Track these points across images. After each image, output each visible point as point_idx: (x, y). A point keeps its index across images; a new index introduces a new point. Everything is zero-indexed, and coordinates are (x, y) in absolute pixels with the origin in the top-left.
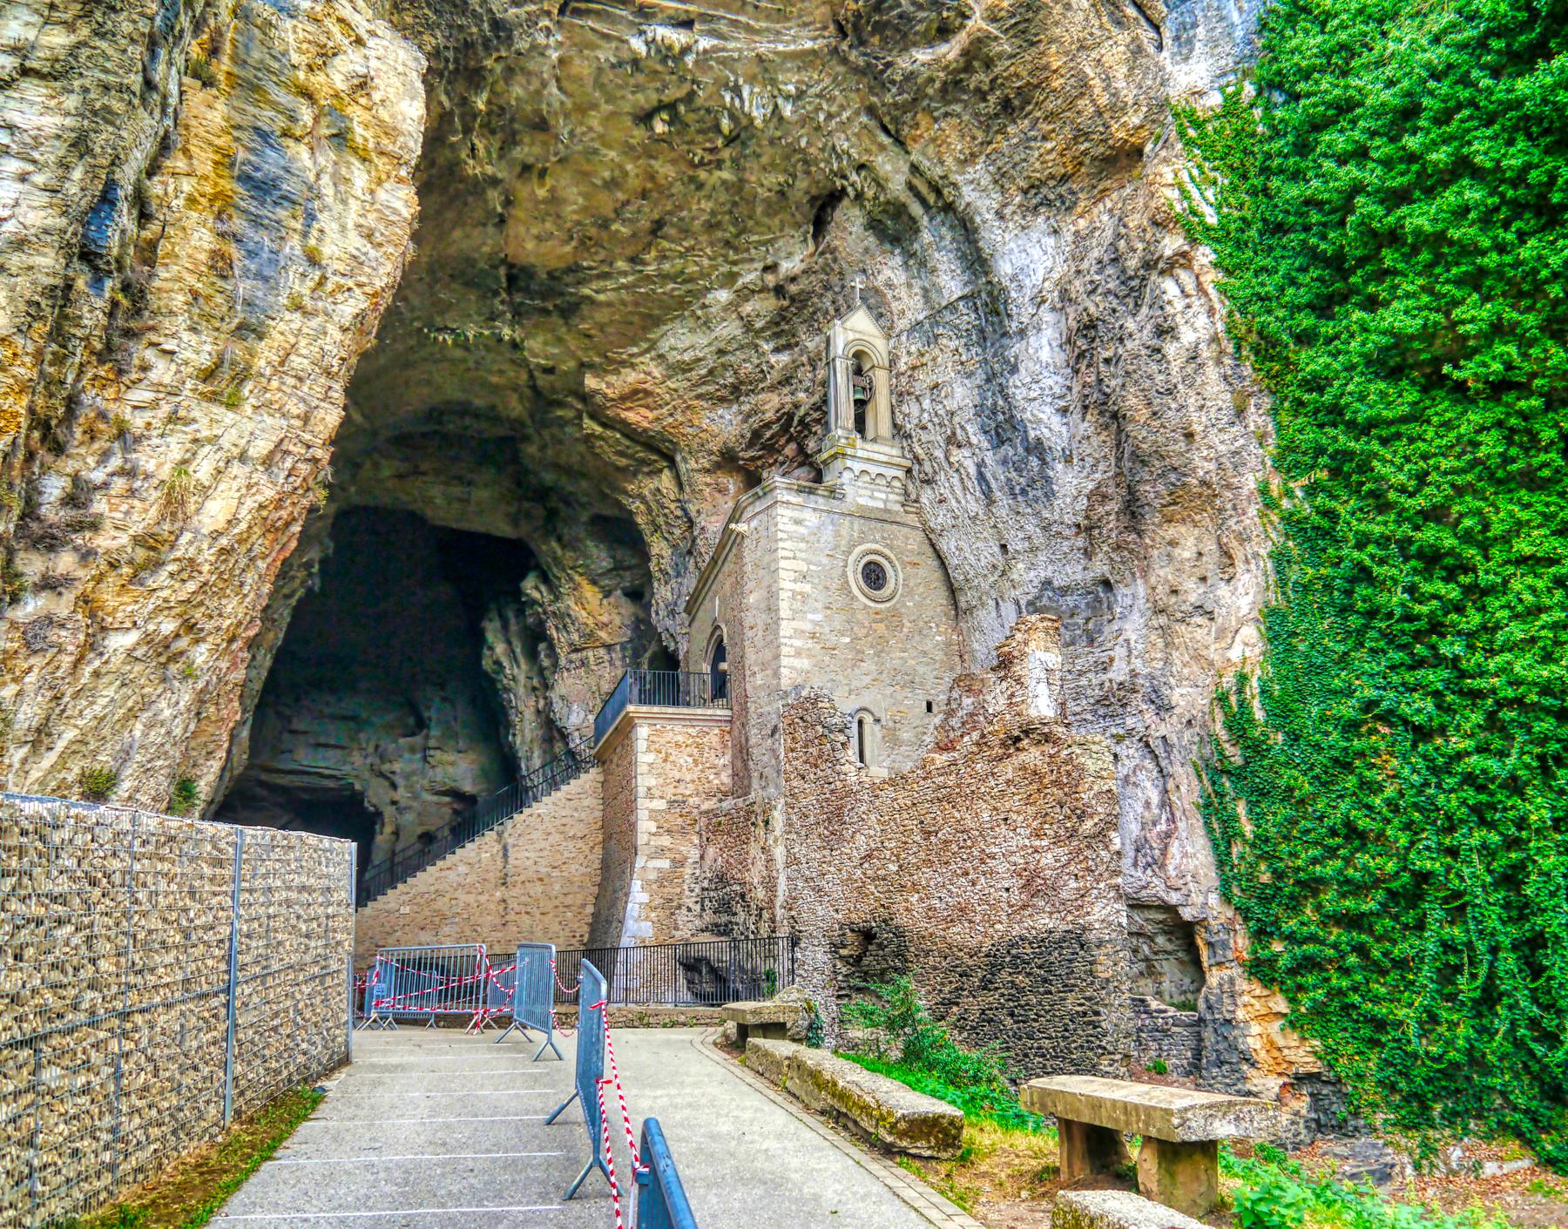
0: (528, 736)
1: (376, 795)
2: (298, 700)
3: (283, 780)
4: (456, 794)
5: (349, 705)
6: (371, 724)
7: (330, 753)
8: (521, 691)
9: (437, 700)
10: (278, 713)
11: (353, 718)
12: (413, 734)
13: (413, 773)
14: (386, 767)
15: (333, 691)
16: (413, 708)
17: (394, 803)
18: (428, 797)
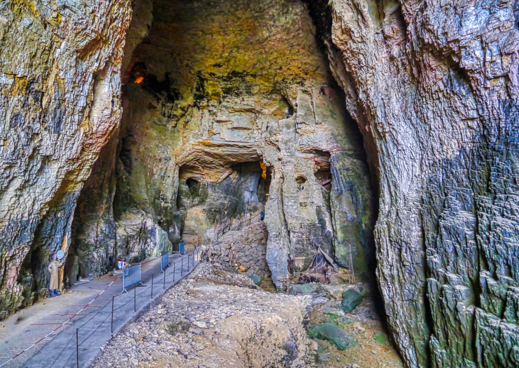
0: (382, 85)
1: (270, 156)
2: (220, 102)
3: (219, 151)
4: (319, 152)
5: (250, 101)
7: (242, 132)
8: (371, 46)
9: (299, 92)
10: (209, 111)
11: (250, 111)
12: (288, 117)
13: (289, 140)
14: (273, 138)
15: (237, 95)
16: (285, 100)
17: (280, 160)
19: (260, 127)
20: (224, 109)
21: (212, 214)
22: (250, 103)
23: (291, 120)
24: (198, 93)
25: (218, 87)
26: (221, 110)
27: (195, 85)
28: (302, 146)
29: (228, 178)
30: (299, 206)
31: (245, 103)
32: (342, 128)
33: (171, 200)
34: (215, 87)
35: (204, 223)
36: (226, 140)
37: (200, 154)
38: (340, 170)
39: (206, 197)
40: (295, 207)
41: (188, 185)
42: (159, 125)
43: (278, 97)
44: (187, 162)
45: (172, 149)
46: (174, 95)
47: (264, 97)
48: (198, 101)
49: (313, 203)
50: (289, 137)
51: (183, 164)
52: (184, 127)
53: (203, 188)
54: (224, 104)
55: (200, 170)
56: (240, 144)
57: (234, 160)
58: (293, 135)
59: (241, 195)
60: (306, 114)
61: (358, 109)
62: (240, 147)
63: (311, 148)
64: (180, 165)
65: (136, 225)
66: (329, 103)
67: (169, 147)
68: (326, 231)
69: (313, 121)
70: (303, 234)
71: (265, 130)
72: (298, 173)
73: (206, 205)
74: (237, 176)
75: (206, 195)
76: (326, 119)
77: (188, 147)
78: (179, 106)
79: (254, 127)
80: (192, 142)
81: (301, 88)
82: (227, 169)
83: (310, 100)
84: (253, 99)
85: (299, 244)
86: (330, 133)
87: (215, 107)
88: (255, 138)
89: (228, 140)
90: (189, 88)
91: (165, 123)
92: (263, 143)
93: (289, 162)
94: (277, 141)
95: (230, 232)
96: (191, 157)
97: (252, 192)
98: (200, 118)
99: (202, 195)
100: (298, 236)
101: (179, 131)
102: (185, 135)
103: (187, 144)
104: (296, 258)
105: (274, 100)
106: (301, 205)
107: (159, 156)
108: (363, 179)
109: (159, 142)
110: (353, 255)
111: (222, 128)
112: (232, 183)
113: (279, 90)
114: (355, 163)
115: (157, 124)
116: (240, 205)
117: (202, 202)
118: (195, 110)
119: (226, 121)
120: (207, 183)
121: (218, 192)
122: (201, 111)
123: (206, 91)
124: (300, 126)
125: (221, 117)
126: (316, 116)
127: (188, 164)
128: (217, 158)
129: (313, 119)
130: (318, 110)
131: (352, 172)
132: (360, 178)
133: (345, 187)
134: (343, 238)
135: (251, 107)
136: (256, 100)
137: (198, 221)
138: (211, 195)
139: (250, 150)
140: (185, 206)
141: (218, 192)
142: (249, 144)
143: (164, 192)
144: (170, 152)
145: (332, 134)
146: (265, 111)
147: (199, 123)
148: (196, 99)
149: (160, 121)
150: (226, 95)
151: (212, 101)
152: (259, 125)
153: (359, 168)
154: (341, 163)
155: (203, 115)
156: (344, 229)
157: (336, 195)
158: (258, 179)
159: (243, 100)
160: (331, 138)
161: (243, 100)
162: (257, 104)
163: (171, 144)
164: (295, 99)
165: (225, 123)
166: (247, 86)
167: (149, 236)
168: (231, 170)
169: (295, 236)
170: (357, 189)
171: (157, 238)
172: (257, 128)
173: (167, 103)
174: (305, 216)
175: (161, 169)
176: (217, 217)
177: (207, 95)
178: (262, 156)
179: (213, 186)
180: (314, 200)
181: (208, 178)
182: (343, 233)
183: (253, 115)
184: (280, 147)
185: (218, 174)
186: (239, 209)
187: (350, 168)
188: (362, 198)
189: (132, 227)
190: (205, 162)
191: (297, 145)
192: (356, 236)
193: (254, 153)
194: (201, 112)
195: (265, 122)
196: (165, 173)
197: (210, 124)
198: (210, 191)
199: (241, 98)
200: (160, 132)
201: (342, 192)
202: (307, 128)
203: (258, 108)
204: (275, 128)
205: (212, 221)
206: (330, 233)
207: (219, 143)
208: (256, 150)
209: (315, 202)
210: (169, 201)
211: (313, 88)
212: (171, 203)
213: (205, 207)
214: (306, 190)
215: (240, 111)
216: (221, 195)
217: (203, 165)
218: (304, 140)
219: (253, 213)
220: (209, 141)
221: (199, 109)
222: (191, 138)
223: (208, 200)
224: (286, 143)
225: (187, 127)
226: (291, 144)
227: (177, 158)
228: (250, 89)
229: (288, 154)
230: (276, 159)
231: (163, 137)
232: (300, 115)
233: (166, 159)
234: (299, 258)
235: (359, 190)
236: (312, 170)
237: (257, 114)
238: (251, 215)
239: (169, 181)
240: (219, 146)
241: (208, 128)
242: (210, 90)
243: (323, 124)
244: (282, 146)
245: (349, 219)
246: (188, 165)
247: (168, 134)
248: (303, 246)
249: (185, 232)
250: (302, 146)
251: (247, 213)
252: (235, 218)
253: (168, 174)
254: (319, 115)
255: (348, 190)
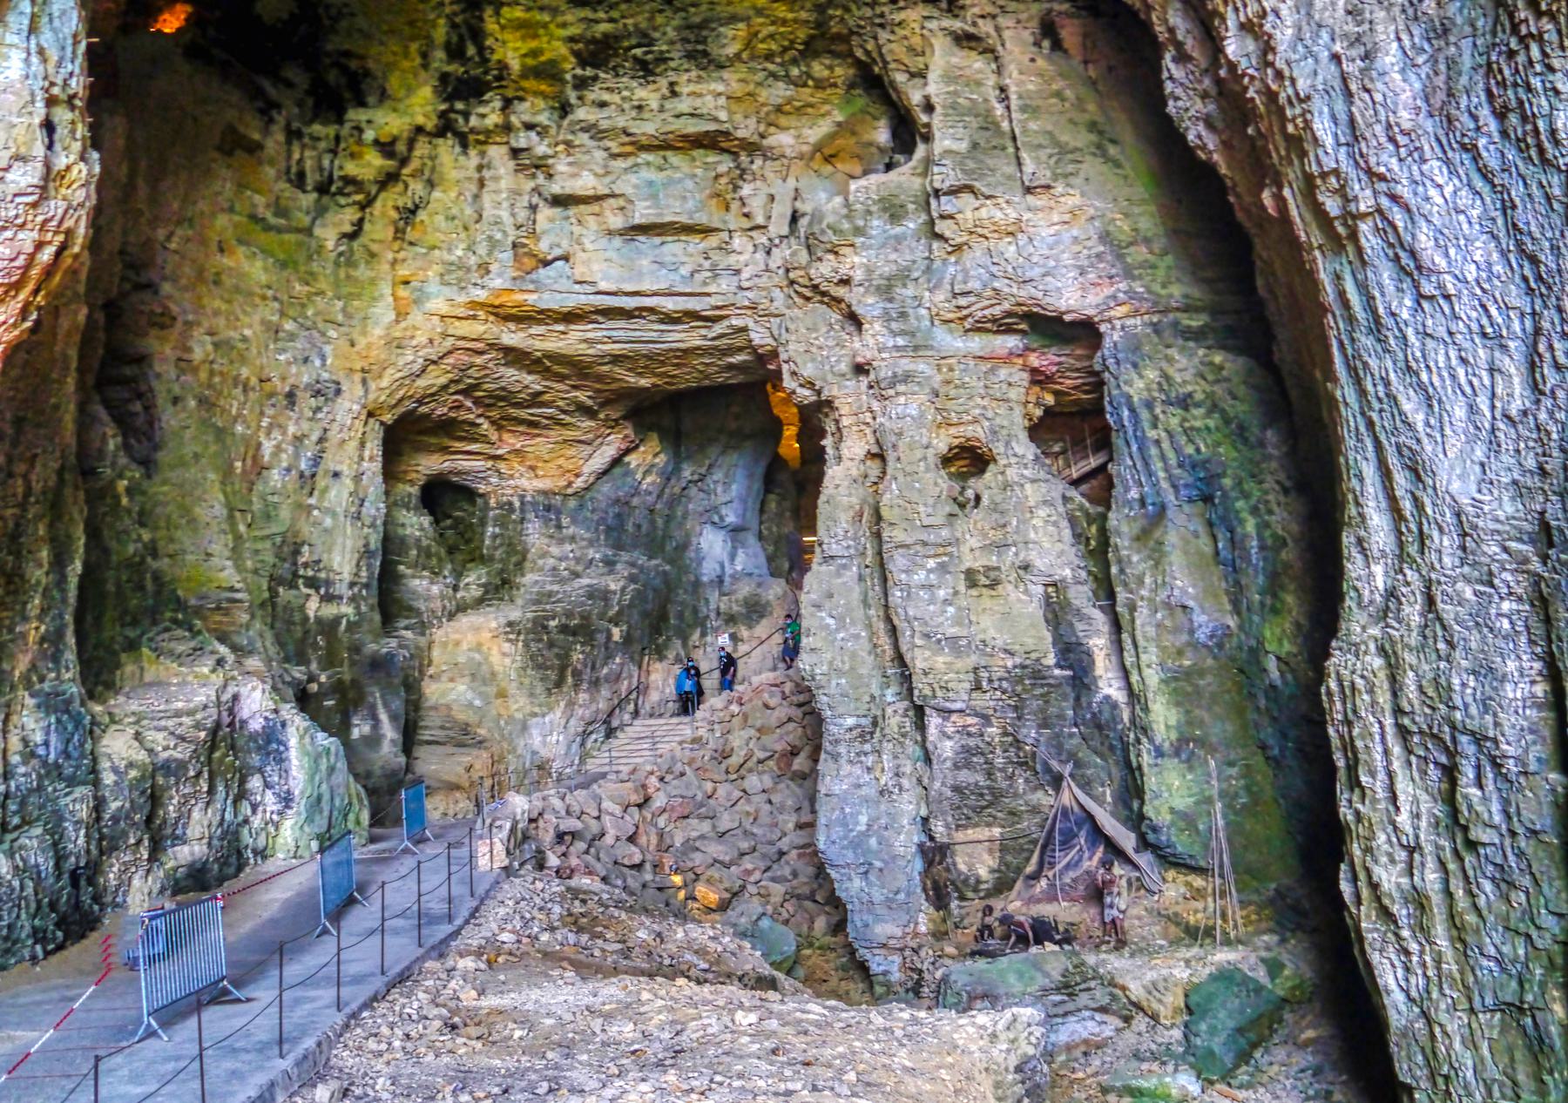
1: (811, 355)
2: (564, 109)
3: (570, 341)
4: (1046, 327)
5: (707, 98)
6: (767, 154)
7: (674, 248)
9: (940, 44)
10: (515, 153)
12: (889, 167)
13: (903, 276)
14: (825, 269)
15: (647, 70)
16: (873, 83)
17: (860, 369)
18: (952, 342)
19: (760, 220)
20: (583, 138)
21: (551, 645)
22: (708, 104)
23: (905, 178)
24: (455, 68)
25: (552, 37)
26: (568, 144)
27: (441, 32)
28: (962, 301)
29: (617, 471)
30: (962, 588)
31: (684, 105)
32: (1153, 208)
33: (352, 585)
34: (535, 36)
35: (512, 689)
36: (603, 286)
37: (479, 360)
38: (1149, 405)
39: (520, 565)
40: (942, 593)
41: (432, 513)
42: (279, 230)
43: (839, 71)
44: (420, 402)
45: (343, 344)
46: (343, 81)
47: (773, 75)
48: (459, 106)
49: (1026, 567)
50: (904, 258)
51: (401, 410)
52: (399, 234)
53: (502, 522)
54: (582, 114)
55: (483, 439)
56: (669, 304)
57: (644, 382)
58: (920, 251)
59: (684, 547)
60: (975, 146)
61: (1220, 108)
62: (670, 319)
63: (1006, 306)
64: (388, 418)
65: (190, 713)
66: (1084, 91)
67: (332, 333)
68: (1098, 698)
69: (1009, 177)
70: (986, 719)
71: (785, 230)
72: (952, 431)
73: (520, 602)
74: (662, 459)
75: (518, 557)
76: (1071, 168)
77: (423, 327)
78: (369, 135)
79: (734, 220)
80: (438, 304)
81: (946, 23)
82: (613, 424)
83: (992, 80)
84: (721, 88)
85: (968, 765)
86: (1092, 231)
87: (543, 132)
88: (738, 272)
89: (613, 288)
90: (414, 47)
91: (307, 220)
92: (777, 293)
93: (907, 378)
94: (845, 282)
95: (638, 727)
96: (436, 378)
97: (736, 531)
98: (474, 188)
99: (498, 554)
100: (964, 731)
101: (373, 255)
102: (403, 272)
103: (416, 317)
104: (960, 836)
105: (820, 85)
106: (972, 584)
107: (283, 379)
108: (1262, 444)
109: (283, 314)
110: (1229, 807)
111: (577, 229)
112: (636, 492)
113: (844, 39)
114: (1221, 368)
115: (268, 228)
116: (682, 596)
117: (500, 588)
118: (447, 149)
119: (598, 198)
120: (522, 497)
121: (573, 539)
122: (473, 152)
123: (495, 57)
124: (947, 204)
125: (577, 175)
126: (1024, 155)
127: (424, 409)
128: (561, 378)
129: (1011, 169)
130: (1033, 126)
131: (1209, 414)
132: (1245, 441)
133: (1174, 487)
134: (1178, 727)
135: (712, 127)
136: (737, 88)
137: (485, 683)
138: (544, 555)
139: (718, 329)
140: (418, 613)
141: (573, 539)
142: (713, 301)
143: (319, 548)
144: (333, 360)
145: (1105, 237)
146: (783, 140)
147: (469, 211)
148: (450, 98)
149: (281, 212)
150: (589, 72)
151: (527, 105)
152: (756, 206)
153: (1242, 391)
154: (1152, 374)
155: (486, 174)
156: (1182, 685)
157: (1136, 528)
158: (760, 470)
159: (674, 94)
160: (1098, 256)
161: (674, 94)
162: (738, 109)
163: (340, 318)
164: (920, 75)
165: (595, 208)
166: (689, 27)
167: (255, 760)
168: (629, 431)
169: (950, 730)
170: (1233, 494)
171: (294, 772)
172: (746, 224)
173: (310, 122)
174: (992, 633)
175: (299, 439)
176: (577, 657)
177: (499, 78)
178: (774, 354)
179: (548, 508)
180: (1033, 556)
181: (521, 471)
182: (1178, 704)
183: (725, 164)
184: (859, 310)
185: (571, 452)
186: (680, 616)
187: (1199, 396)
188: (1260, 538)
189: (170, 723)
190: (505, 397)
191: (940, 296)
192: (1240, 712)
193: (739, 342)
194: (474, 159)
195: (784, 190)
196: (317, 460)
197: (522, 215)
198: (535, 535)
199: (663, 83)
200: (284, 265)
201: (1162, 508)
202: (984, 213)
203: (746, 129)
204: (830, 219)
205: (553, 675)
206: (1115, 706)
207: (570, 302)
208: (744, 329)
209: (1039, 563)
210: (342, 589)
211: (1001, 21)
212: (353, 599)
213: (515, 614)
214: (995, 508)
215: (663, 145)
216: (591, 553)
217: (494, 414)
218: (974, 268)
219: (744, 632)
220: (520, 297)
221: (465, 146)
222: (433, 287)
223: (529, 578)
224: (889, 288)
225: (411, 234)
226: (910, 291)
227: (373, 386)
228: (704, 41)
229: (900, 341)
230: (844, 367)
231: (298, 287)
232: (948, 152)
233: (318, 393)
234: (971, 834)
235: (1246, 496)
236: (1018, 411)
237: (744, 158)
238: (734, 638)
239: (338, 495)
240: (571, 317)
241: (512, 234)
242: (511, 51)
243: (1059, 188)
244: (867, 304)
245: (1201, 635)
246: (427, 416)
247: (324, 269)
248: (989, 775)
249: (425, 735)
250: (962, 301)
251: (716, 630)
252: (661, 658)
253: (330, 463)
254: (1040, 146)
255: (1190, 501)
